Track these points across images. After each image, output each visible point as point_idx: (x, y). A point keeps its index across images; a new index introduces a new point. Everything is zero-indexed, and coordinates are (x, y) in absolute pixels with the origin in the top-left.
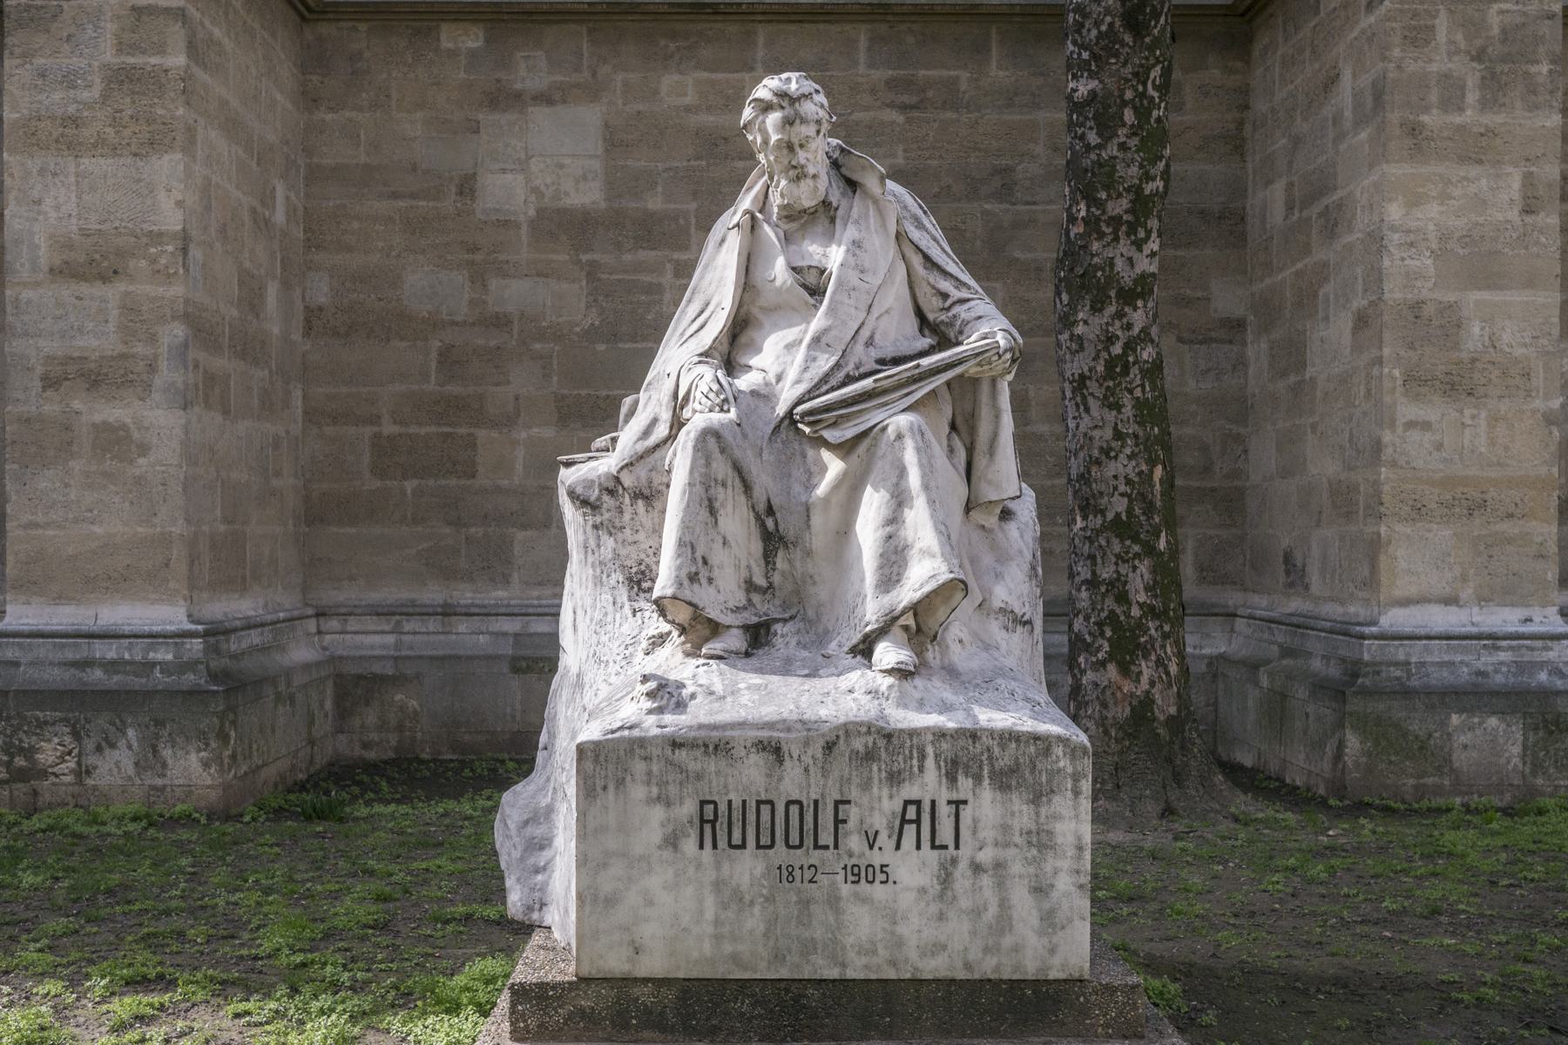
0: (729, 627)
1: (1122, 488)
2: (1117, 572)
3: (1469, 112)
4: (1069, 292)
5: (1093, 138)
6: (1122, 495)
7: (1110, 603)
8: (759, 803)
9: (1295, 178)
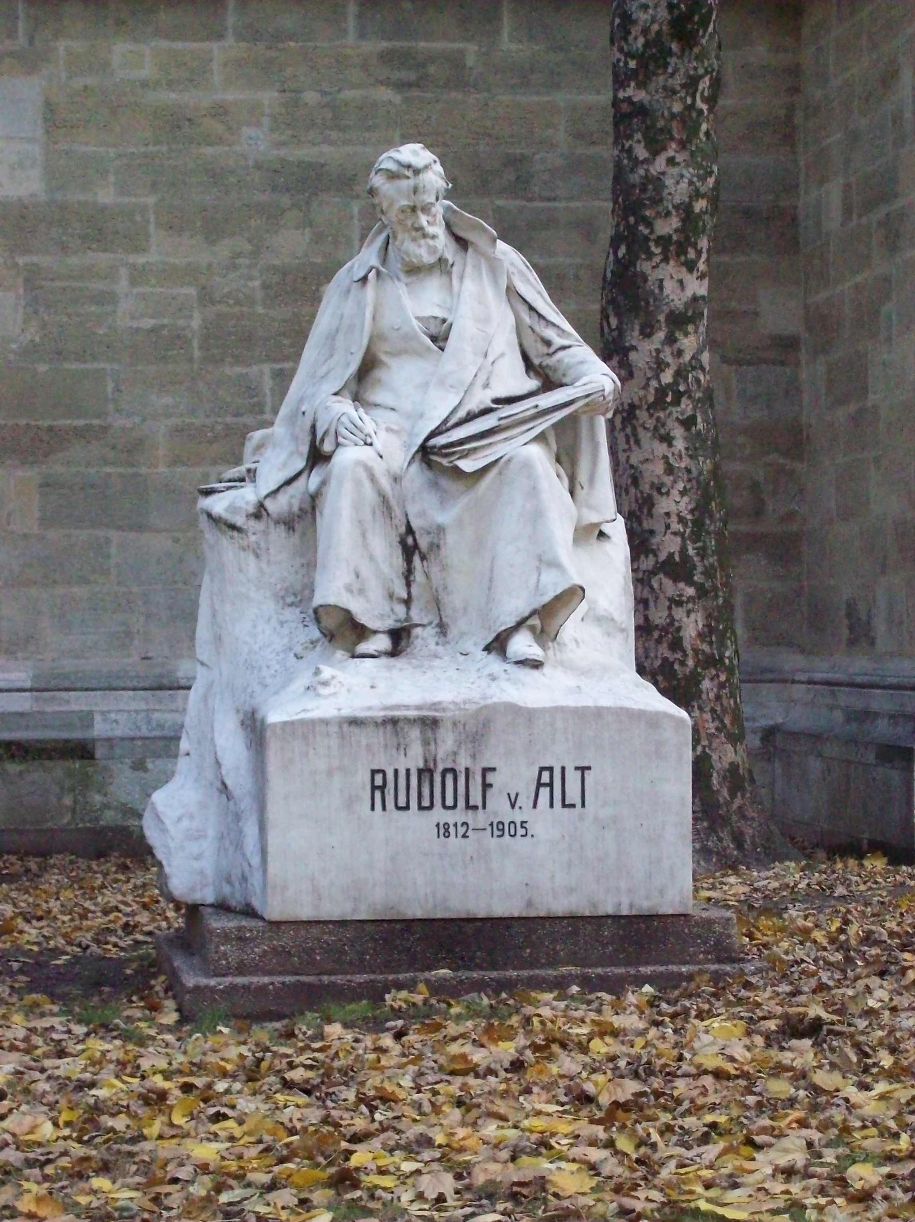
0: (375, 632)
1: (676, 526)
2: (670, 616)
4: (618, 315)
5: (641, 152)
6: (675, 534)
7: (664, 651)
8: (420, 772)
9: (853, 179)
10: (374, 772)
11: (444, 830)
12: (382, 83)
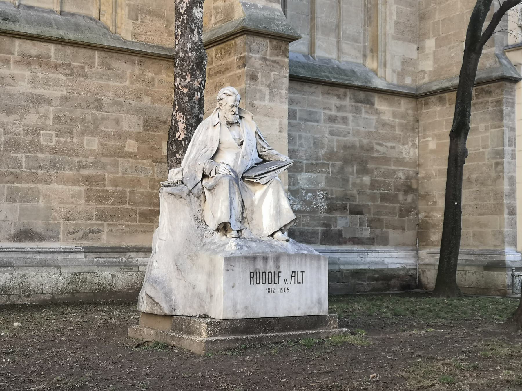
3: (266, 102)
10: (251, 272)
11: (268, 290)
12: (61, 73)
